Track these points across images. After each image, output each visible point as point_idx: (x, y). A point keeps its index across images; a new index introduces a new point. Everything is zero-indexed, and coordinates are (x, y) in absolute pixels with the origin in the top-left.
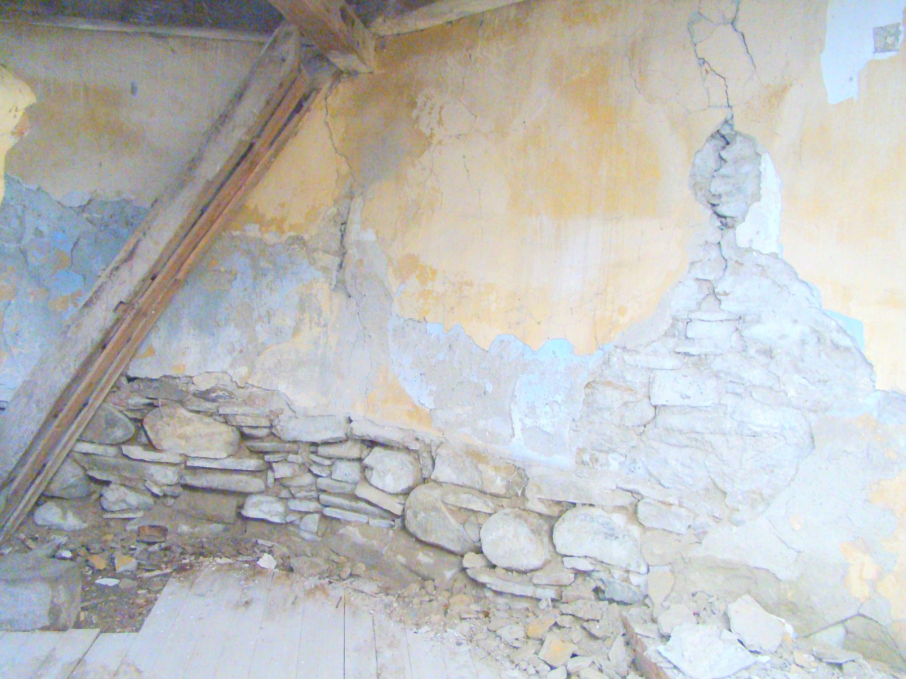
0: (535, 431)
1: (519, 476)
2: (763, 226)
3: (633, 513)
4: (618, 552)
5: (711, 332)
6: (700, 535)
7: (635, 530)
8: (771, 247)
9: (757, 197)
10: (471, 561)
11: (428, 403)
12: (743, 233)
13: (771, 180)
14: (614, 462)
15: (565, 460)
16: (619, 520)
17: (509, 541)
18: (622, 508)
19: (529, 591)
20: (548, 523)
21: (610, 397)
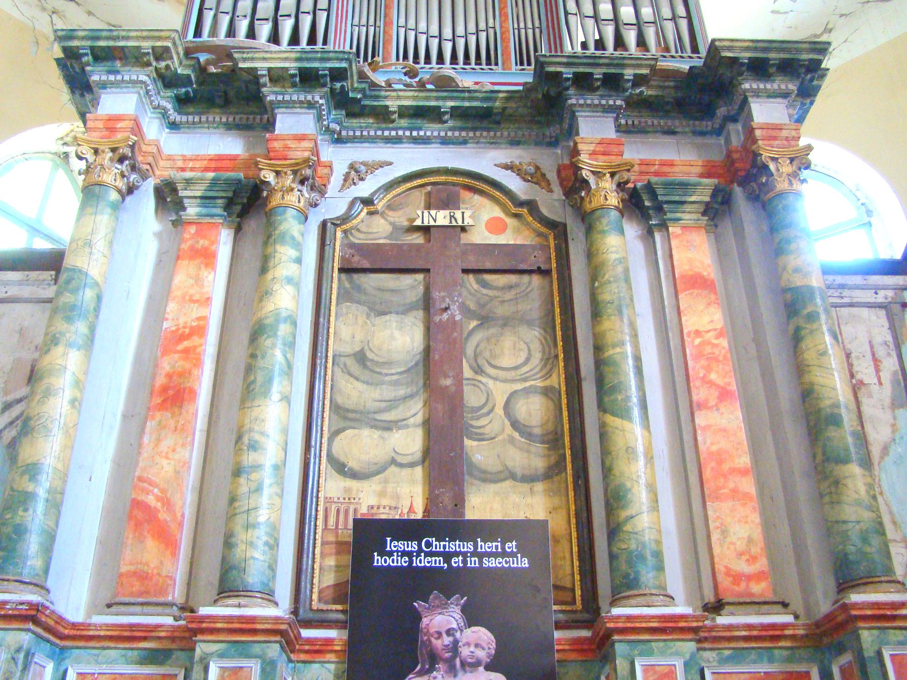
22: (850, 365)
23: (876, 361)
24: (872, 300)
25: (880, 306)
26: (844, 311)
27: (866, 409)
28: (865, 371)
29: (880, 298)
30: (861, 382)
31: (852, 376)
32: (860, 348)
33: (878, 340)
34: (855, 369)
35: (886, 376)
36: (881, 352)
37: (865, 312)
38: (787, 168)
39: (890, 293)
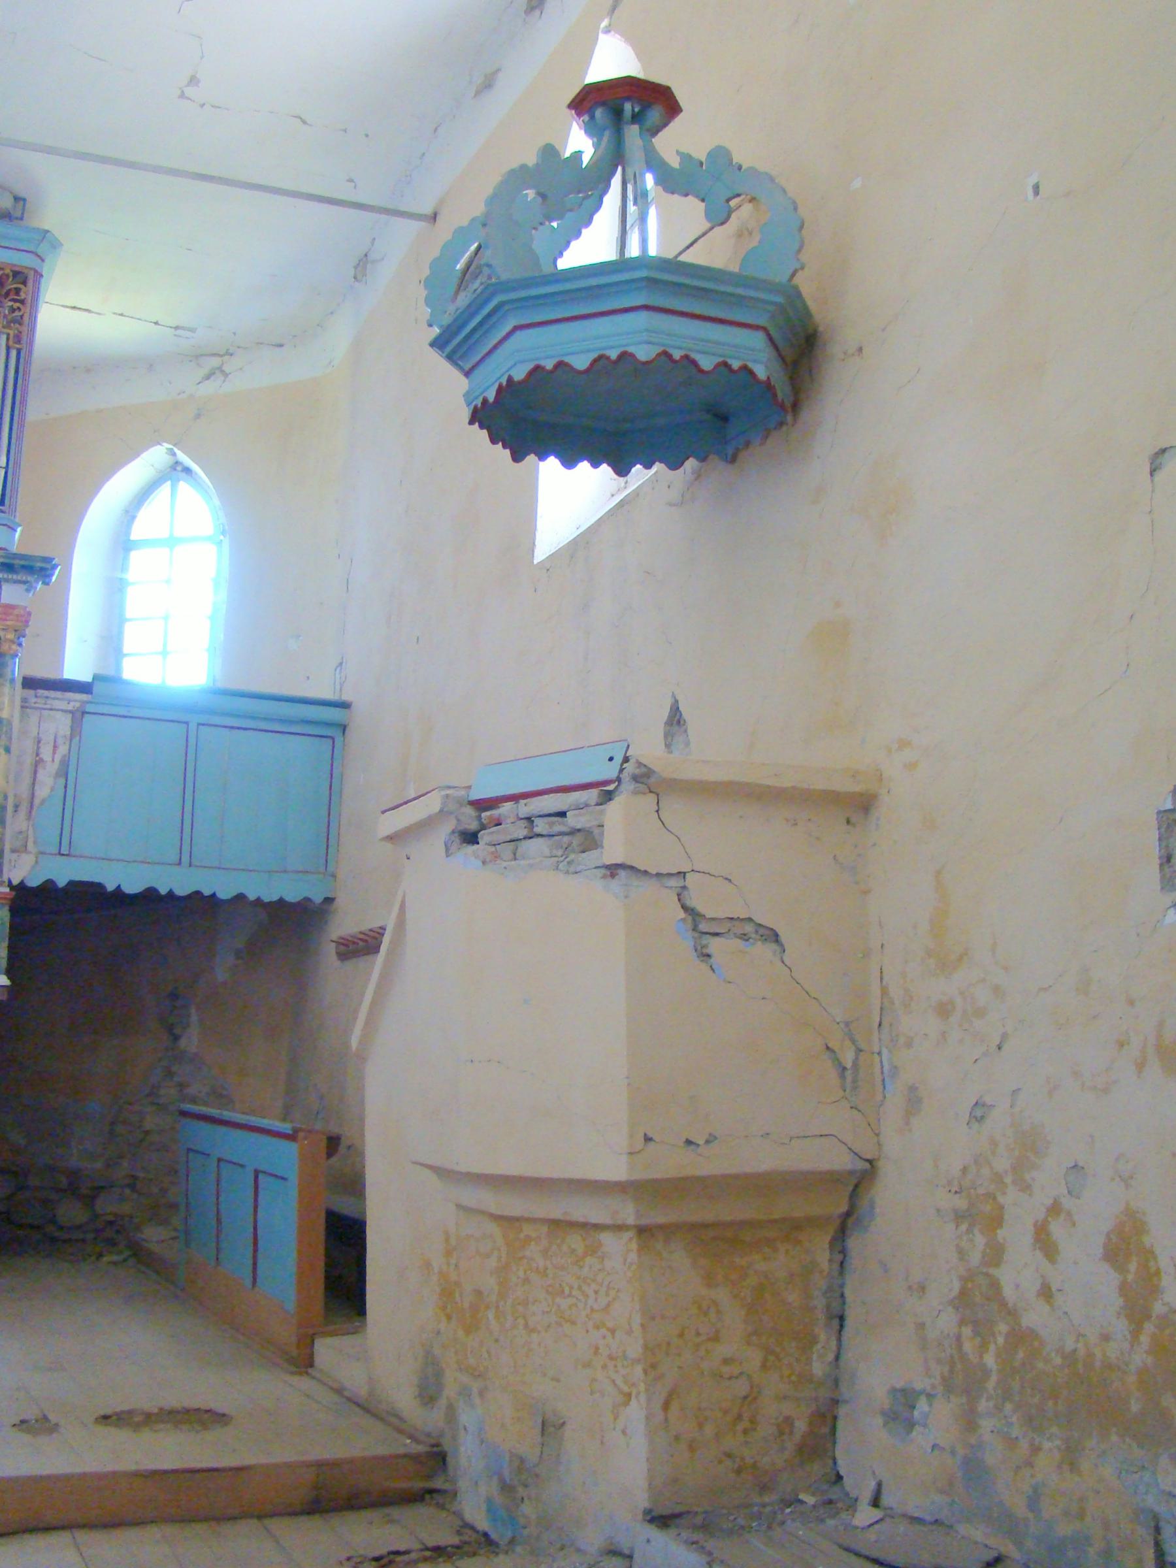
0: (82, 1152)
1: (74, 1175)
2: (191, 1041)
3: (133, 1187)
4: (126, 1208)
5: (169, 1092)
6: (164, 1191)
7: (135, 1196)
8: (194, 1050)
9: (188, 1025)
10: (50, 1229)
11: (23, 1142)
12: (183, 1043)
13: (194, 1018)
14: (125, 1164)
15: (99, 1164)
16: (127, 1191)
17: (71, 1213)
18: (128, 1185)
19: (81, 1236)
20: (90, 1200)
21: (119, 1129)
22: (38, 748)
23: (55, 747)
24: (64, 708)
25: (70, 712)
26: (46, 713)
27: (41, 775)
28: (46, 753)
29: (70, 707)
30: (42, 760)
31: (37, 755)
32: (48, 739)
33: (61, 733)
34: (42, 750)
35: (58, 758)
36: (60, 741)
37: (59, 715)
38: (11, 636)
39: (78, 705)
